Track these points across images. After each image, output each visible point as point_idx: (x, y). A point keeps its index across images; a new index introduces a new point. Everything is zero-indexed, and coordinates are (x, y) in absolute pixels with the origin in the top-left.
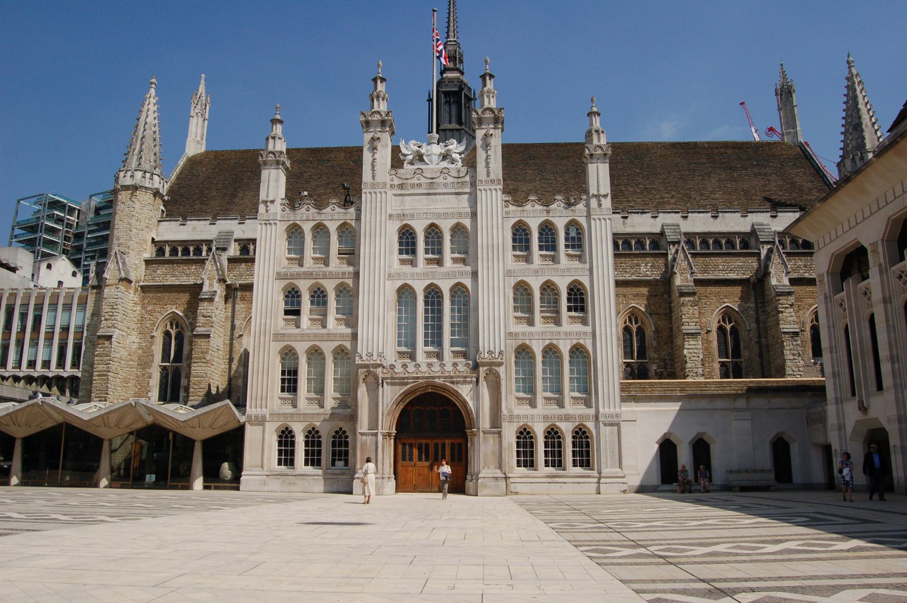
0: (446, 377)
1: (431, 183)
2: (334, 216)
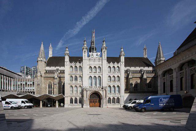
2: (78, 65)
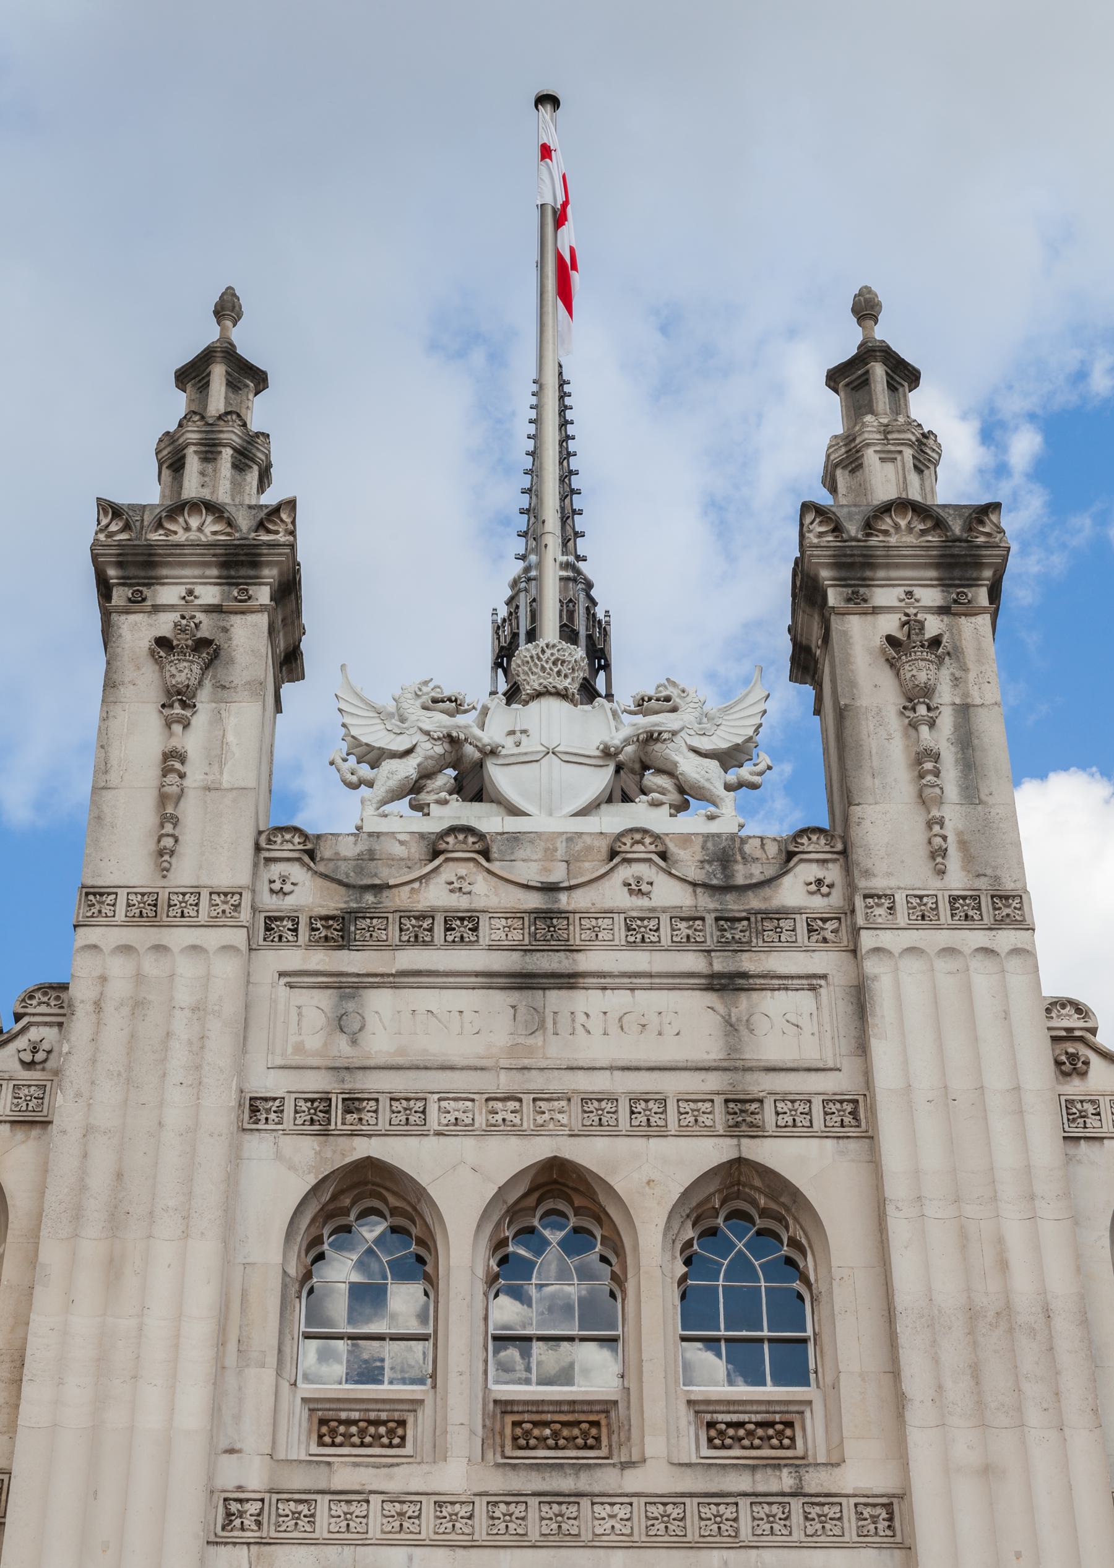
1: (546, 916)
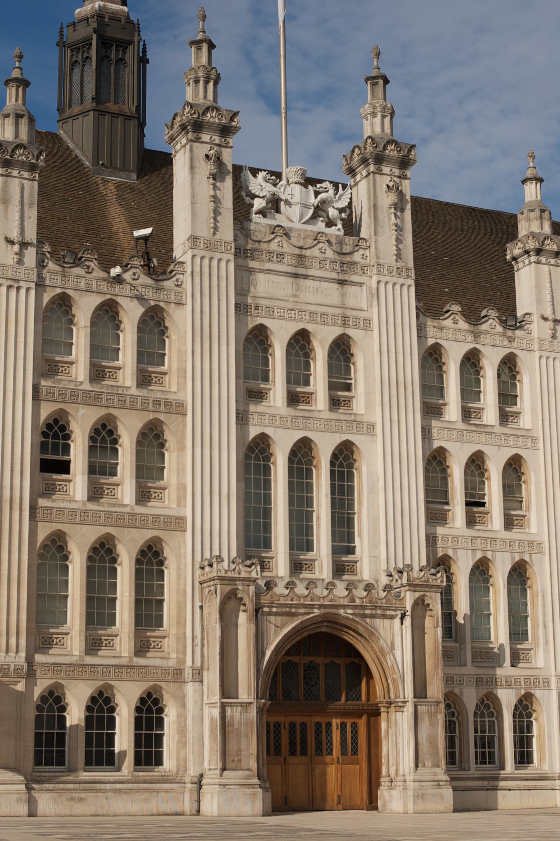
0: (355, 607)
1: (301, 257)
